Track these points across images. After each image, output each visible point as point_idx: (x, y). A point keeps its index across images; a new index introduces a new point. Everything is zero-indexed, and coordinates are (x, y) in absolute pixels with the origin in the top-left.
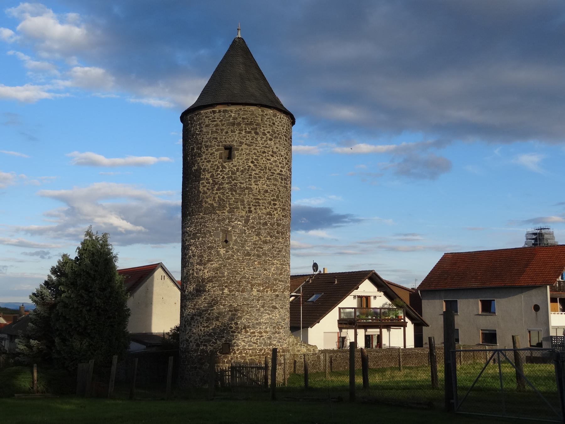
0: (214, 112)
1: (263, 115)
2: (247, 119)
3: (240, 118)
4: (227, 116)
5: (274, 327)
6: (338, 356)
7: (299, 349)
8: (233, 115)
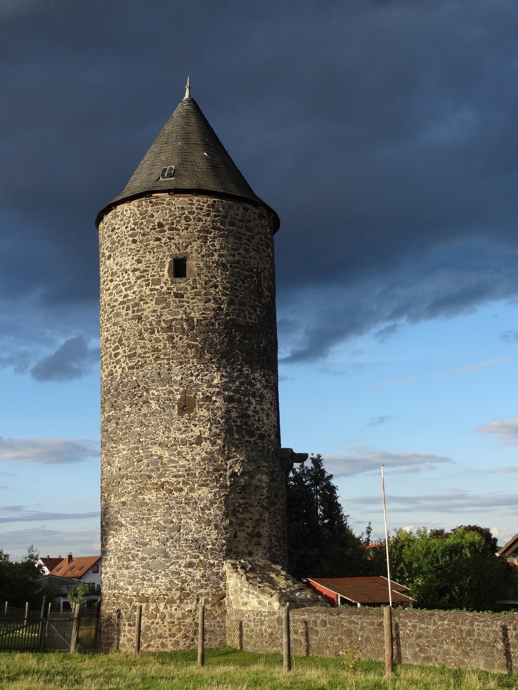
5: (119, 558)
6: (319, 621)
7: (245, 600)
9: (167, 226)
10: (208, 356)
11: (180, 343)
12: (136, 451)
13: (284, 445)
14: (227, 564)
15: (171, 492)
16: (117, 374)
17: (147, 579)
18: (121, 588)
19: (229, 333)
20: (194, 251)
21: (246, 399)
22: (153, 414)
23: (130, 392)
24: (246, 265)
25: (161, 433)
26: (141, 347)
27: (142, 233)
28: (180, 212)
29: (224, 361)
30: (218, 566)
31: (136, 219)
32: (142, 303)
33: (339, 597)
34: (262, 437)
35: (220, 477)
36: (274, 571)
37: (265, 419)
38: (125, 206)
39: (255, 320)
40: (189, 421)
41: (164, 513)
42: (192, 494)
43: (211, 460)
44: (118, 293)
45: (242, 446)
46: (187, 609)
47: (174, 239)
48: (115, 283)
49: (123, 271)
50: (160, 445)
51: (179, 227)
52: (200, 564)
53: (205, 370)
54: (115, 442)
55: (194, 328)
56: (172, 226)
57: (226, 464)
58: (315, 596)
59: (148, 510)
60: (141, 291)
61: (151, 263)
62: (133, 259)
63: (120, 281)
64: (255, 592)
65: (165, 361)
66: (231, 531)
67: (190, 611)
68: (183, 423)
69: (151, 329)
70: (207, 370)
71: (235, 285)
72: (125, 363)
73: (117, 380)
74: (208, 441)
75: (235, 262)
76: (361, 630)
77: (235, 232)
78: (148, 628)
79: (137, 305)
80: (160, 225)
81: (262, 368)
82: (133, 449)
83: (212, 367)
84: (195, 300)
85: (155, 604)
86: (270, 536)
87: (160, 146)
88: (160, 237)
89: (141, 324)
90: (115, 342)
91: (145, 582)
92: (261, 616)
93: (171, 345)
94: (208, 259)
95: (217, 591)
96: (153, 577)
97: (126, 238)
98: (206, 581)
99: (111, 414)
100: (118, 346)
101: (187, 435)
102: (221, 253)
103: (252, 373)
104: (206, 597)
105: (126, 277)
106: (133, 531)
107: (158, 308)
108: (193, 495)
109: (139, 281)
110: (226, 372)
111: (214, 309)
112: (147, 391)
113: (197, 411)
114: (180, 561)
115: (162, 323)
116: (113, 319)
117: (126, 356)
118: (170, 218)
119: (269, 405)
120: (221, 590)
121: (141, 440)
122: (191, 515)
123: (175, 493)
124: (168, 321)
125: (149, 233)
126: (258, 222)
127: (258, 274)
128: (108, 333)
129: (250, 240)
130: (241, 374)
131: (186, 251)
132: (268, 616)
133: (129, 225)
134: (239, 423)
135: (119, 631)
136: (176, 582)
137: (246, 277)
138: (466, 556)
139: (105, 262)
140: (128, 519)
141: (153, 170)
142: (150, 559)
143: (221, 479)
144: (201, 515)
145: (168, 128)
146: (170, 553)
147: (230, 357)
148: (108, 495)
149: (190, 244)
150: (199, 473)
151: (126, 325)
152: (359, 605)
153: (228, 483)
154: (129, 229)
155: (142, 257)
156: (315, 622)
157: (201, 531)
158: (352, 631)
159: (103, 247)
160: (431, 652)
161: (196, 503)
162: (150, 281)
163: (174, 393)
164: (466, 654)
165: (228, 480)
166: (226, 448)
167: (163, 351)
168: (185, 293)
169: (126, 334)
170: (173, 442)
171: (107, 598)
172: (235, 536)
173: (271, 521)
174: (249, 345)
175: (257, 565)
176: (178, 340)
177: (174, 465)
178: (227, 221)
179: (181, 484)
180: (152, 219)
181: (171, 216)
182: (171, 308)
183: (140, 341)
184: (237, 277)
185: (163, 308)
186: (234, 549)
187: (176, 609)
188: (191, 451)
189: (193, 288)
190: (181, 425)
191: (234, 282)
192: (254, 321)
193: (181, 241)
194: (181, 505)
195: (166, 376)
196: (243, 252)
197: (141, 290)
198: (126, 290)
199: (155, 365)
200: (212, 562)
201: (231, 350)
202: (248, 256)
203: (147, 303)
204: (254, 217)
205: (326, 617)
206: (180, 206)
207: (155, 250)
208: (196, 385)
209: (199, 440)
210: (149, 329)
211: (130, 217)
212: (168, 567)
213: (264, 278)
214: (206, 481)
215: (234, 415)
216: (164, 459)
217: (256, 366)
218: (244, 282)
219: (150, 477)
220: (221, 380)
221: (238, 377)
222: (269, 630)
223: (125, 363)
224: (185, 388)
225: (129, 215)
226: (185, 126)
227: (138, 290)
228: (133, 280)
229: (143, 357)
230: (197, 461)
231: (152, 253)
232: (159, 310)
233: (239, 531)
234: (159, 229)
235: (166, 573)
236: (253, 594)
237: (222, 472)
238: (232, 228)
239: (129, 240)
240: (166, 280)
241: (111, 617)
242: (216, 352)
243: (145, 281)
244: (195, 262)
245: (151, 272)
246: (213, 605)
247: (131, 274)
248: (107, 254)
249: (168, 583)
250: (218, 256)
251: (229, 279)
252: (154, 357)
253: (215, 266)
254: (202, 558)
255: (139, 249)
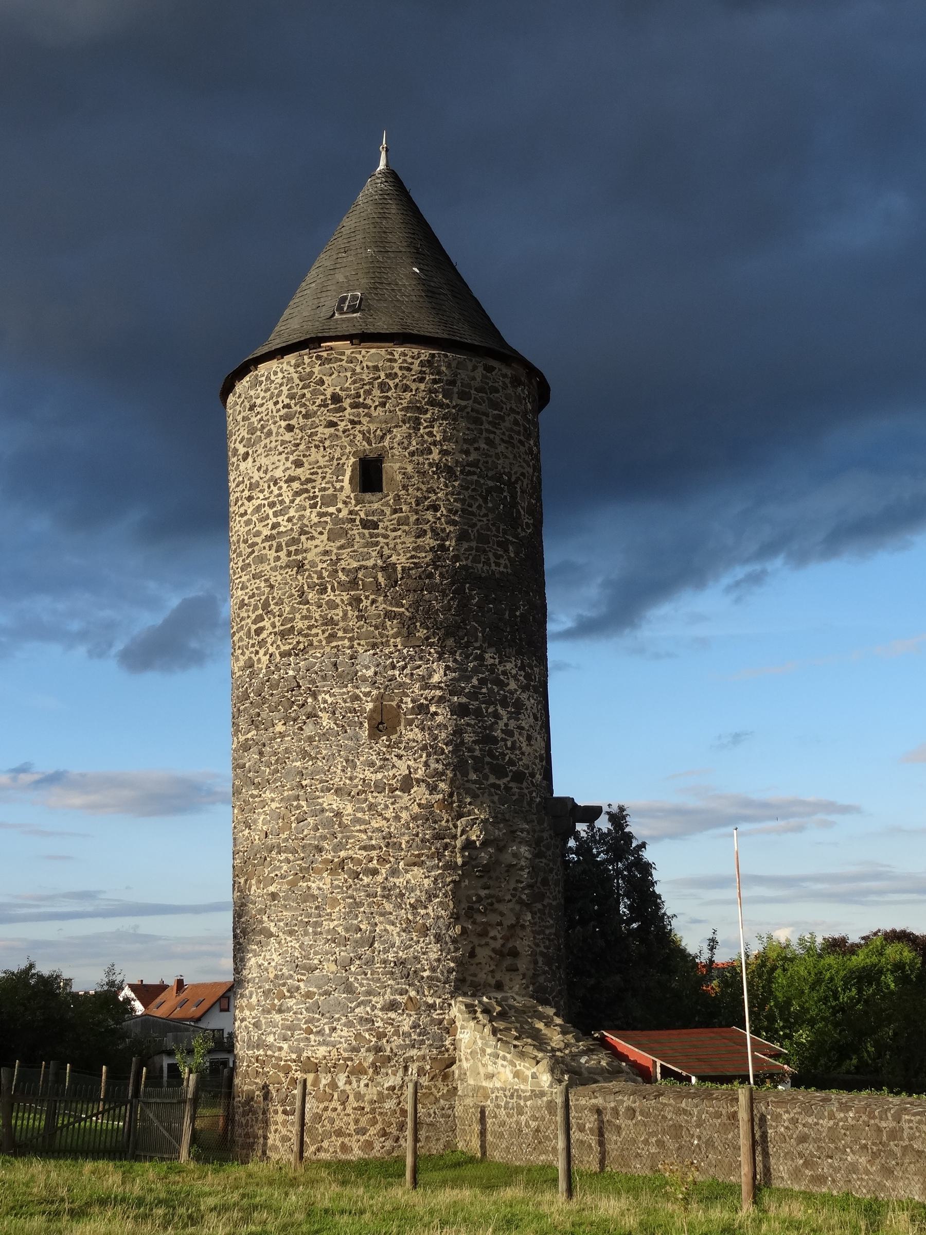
5: (266, 993)
6: (622, 1110)
7: (490, 1069)
9: (348, 401)
10: (422, 633)
11: (372, 610)
12: (295, 803)
13: (557, 793)
14: (458, 1004)
15: (356, 875)
16: (260, 666)
17: (314, 1030)
18: (270, 1047)
19: (459, 592)
20: (396, 445)
21: (490, 710)
22: (324, 736)
23: (284, 696)
24: (488, 469)
25: (339, 771)
26: (303, 617)
27: (304, 412)
28: (371, 375)
29: (450, 642)
30: (441, 1008)
31: (292, 388)
32: (303, 538)
33: (658, 1065)
34: (519, 777)
35: (445, 850)
36: (541, 1017)
37: (524, 745)
38: (273, 364)
39: (506, 567)
40: (389, 750)
41: (344, 913)
42: (395, 880)
43: (427, 820)
44: (261, 520)
45: (483, 794)
46: (386, 1085)
47: (360, 423)
48: (256, 502)
49: (269, 480)
50: (338, 791)
51: (368, 402)
52: (410, 1005)
53: (417, 658)
54: (257, 786)
55: (396, 582)
56: (357, 400)
57: (456, 827)
58: (615, 1063)
59: (317, 908)
60: (302, 517)
61: (320, 467)
62: (287, 459)
63: (265, 499)
64: (508, 1056)
65: (346, 641)
66: (463, 945)
67: (393, 1088)
68: (379, 754)
69: (321, 585)
70: (421, 659)
71: (471, 507)
72: (275, 646)
73: (261, 676)
74: (423, 785)
75: (469, 464)
76: (699, 1125)
77: (469, 409)
78: (318, 1118)
79: (295, 541)
80: (336, 398)
81: (519, 653)
82: (289, 799)
83: (430, 653)
84: (399, 533)
85: (329, 1075)
86: (534, 954)
87: (335, 257)
88: (335, 420)
89: (303, 575)
90: (256, 608)
91: (312, 1037)
92: (519, 1097)
93: (356, 613)
94: (421, 459)
95: (440, 1052)
96: (327, 1028)
97: (275, 423)
98: (419, 1035)
99: (249, 736)
100: (261, 615)
101: (386, 774)
102: (445, 448)
103: (500, 663)
104: (420, 1064)
105: (276, 492)
106: (289, 944)
107: (333, 546)
108: (397, 881)
109: (298, 499)
110: (455, 661)
111: (432, 549)
112: (314, 695)
113: (404, 732)
114: (374, 999)
115: (340, 574)
116: (253, 567)
117: (275, 634)
118: (352, 387)
119: (532, 720)
120: (447, 1050)
121: (304, 783)
122: (392, 918)
123: (365, 878)
124: (350, 571)
125: (315, 413)
126: (510, 391)
127: (511, 485)
128: (243, 592)
129: (496, 424)
130: (481, 665)
131: (381, 444)
132: (530, 1098)
133: (280, 400)
134: (477, 753)
135: (266, 1122)
136: (367, 1036)
137: (489, 491)
138: (888, 987)
139: (238, 465)
140: (282, 924)
141: (322, 300)
142: (320, 995)
143: (446, 853)
144: (411, 917)
145: (349, 223)
146: (356, 985)
147: (461, 634)
148: (246, 881)
149: (390, 431)
150: (408, 842)
151: (277, 578)
152: (694, 1079)
153: (459, 861)
154: (280, 405)
155: (304, 456)
156: (615, 1111)
157: (411, 946)
158: (681, 1126)
159: (234, 438)
160: (824, 1168)
161: (402, 895)
162: (318, 499)
163: (361, 700)
164: (888, 1172)
165: (458, 855)
166: (455, 798)
167: (341, 624)
168: (380, 521)
169: (275, 594)
170: (360, 787)
171: (245, 1064)
172: (472, 954)
173: (537, 928)
174: (495, 613)
175: (511, 1007)
176: (368, 604)
177: (362, 827)
178: (456, 390)
179: (375, 862)
180: (321, 389)
181: (354, 382)
182: (356, 547)
183: (301, 606)
184: (473, 490)
185: (342, 547)
186: (469, 978)
187: (367, 1085)
188: (393, 804)
189: (395, 511)
190: (374, 757)
191: (468, 500)
192: (505, 570)
193: (373, 427)
194: (375, 900)
195: (347, 669)
196: (483, 446)
197: (303, 516)
198: (276, 515)
199: (328, 649)
200: (430, 1000)
201: (463, 621)
202: (492, 452)
203: (313, 538)
204: (504, 383)
205: (635, 1102)
206: (370, 364)
207: (327, 443)
208: (401, 685)
209: (407, 784)
210: (317, 584)
211: (281, 385)
212: (353, 1010)
213: (523, 492)
214: (419, 856)
215: (468, 738)
216: (345, 817)
217: (507, 650)
218: (485, 500)
219: (320, 850)
220: (445, 675)
221: (475, 671)
222: (533, 1124)
223: (275, 646)
224: (382, 691)
225: (279, 381)
226: (379, 220)
227: (297, 515)
228: (287, 497)
229: (306, 636)
230: (403, 822)
231: (322, 449)
232: (335, 551)
233: (479, 945)
234: (333, 406)
235: (349, 1021)
236: (504, 1058)
237: (448, 840)
238: (463, 403)
239: (280, 426)
240: (347, 497)
241: (253, 1098)
242: (437, 626)
243: (310, 498)
244: (398, 465)
245: (320, 483)
246: (432, 1078)
247: (285, 486)
248: (242, 450)
249: (352, 1039)
250: (440, 453)
251: (459, 494)
252: (326, 634)
253: (433, 472)
254: (413, 993)
255: (298, 441)
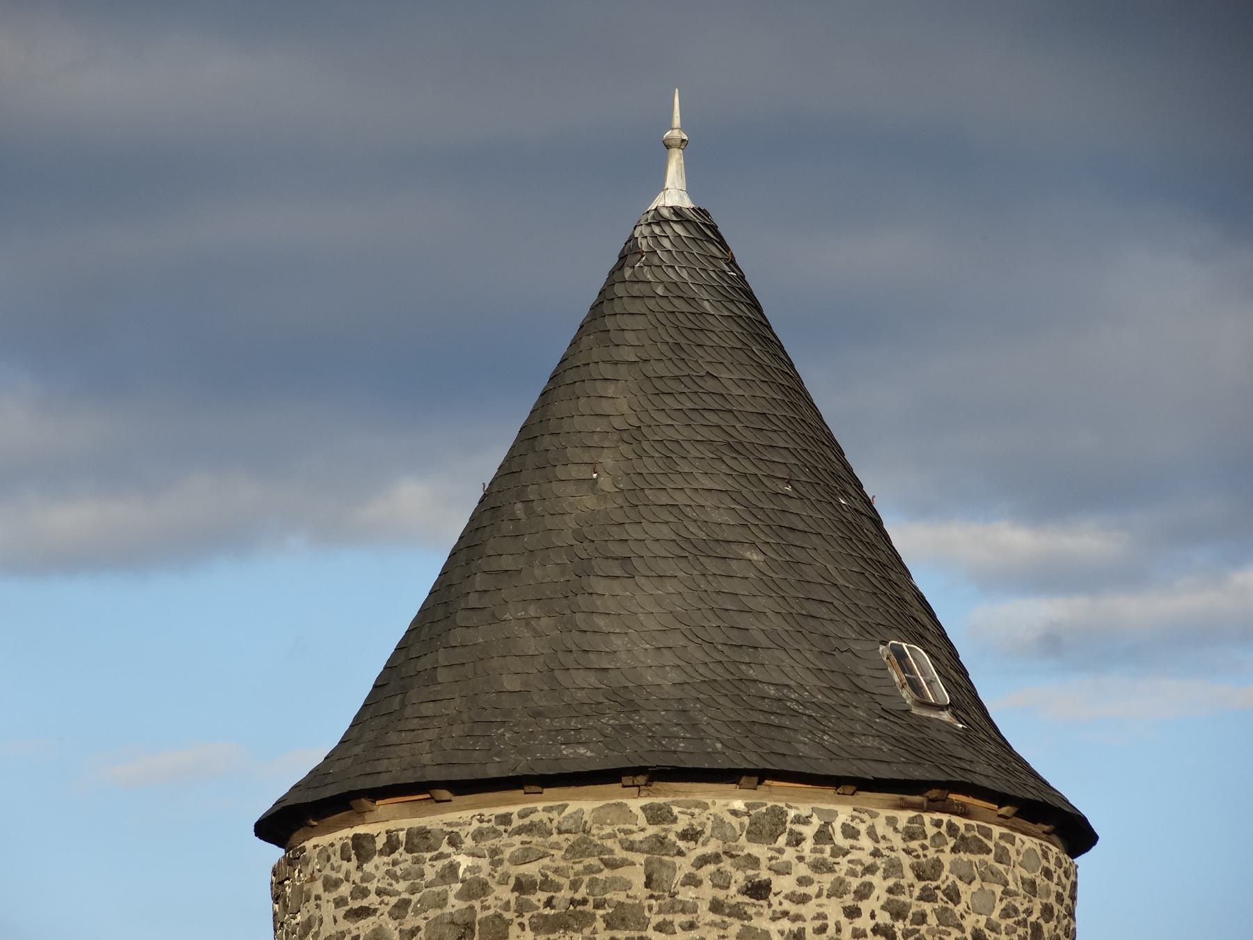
0: (361, 848)
1: (660, 843)
2: (546, 884)
3: (503, 881)
4: (430, 873)
8: (464, 862)
118: (1004, 923)
133: (865, 906)
181: (1006, 914)
206: (1027, 875)
211: (870, 870)
225: (869, 860)
